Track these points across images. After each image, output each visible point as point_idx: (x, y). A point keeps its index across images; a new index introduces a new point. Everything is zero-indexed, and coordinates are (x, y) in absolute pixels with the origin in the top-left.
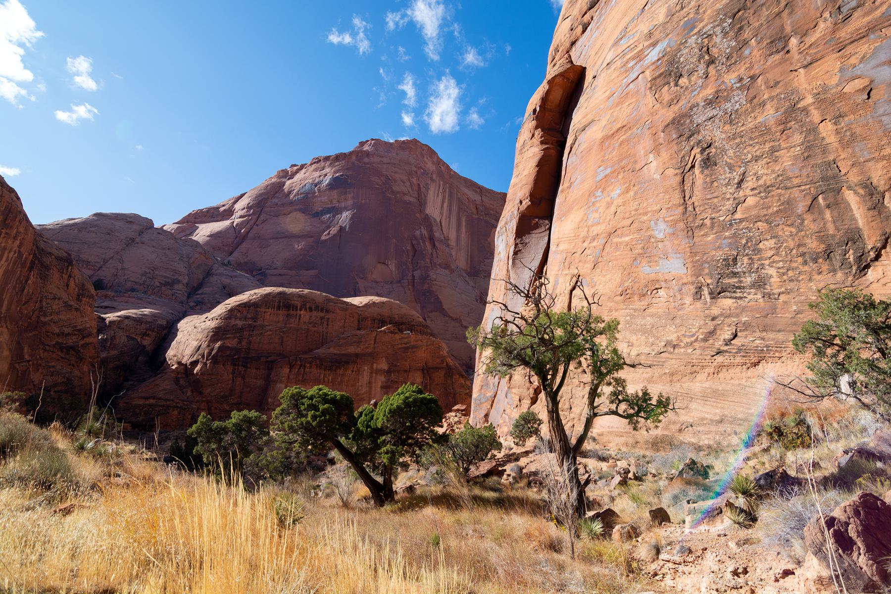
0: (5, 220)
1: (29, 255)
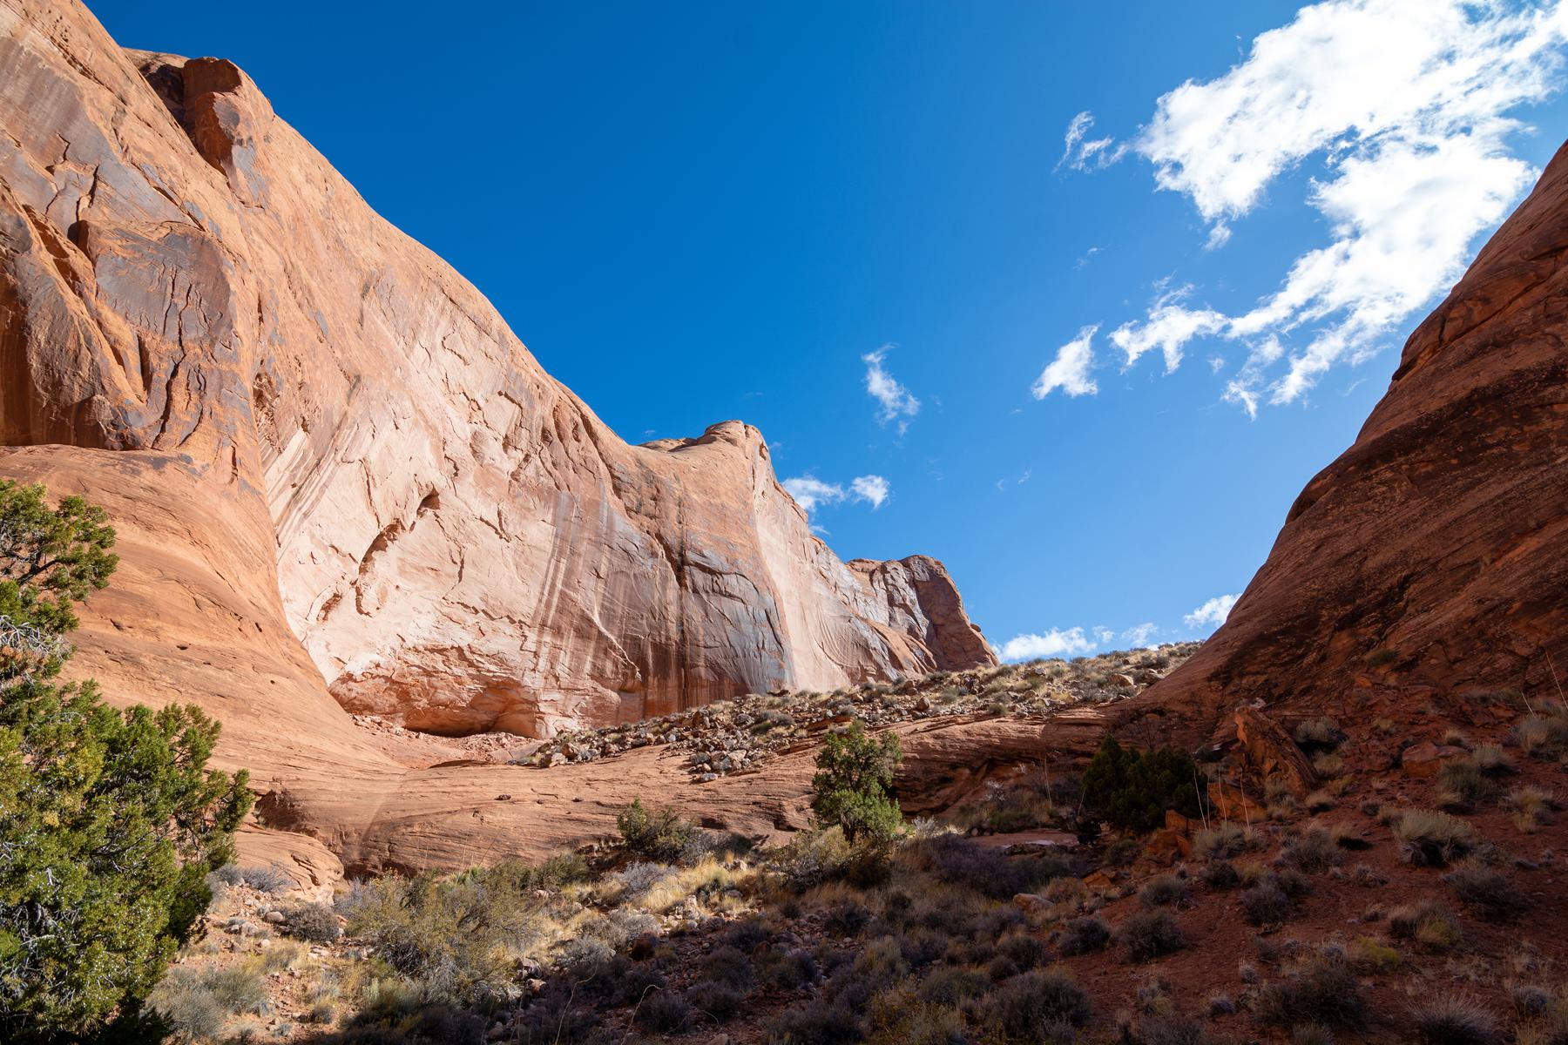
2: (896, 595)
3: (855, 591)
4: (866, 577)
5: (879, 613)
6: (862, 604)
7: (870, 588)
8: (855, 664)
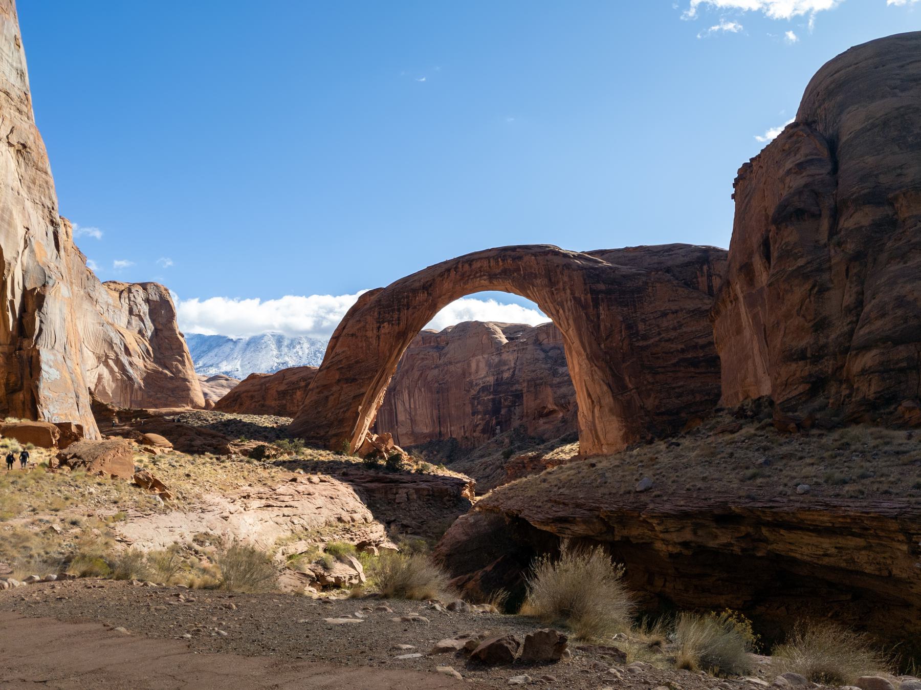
0: (550, 280)
1: (586, 295)
2: (135, 308)
3: (108, 305)
4: (117, 295)
5: (122, 319)
6: (112, 313)
7: (118, 302)
8: (102, 352)
